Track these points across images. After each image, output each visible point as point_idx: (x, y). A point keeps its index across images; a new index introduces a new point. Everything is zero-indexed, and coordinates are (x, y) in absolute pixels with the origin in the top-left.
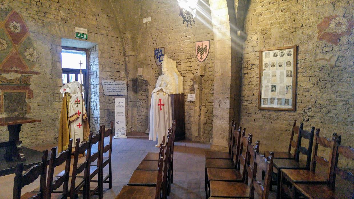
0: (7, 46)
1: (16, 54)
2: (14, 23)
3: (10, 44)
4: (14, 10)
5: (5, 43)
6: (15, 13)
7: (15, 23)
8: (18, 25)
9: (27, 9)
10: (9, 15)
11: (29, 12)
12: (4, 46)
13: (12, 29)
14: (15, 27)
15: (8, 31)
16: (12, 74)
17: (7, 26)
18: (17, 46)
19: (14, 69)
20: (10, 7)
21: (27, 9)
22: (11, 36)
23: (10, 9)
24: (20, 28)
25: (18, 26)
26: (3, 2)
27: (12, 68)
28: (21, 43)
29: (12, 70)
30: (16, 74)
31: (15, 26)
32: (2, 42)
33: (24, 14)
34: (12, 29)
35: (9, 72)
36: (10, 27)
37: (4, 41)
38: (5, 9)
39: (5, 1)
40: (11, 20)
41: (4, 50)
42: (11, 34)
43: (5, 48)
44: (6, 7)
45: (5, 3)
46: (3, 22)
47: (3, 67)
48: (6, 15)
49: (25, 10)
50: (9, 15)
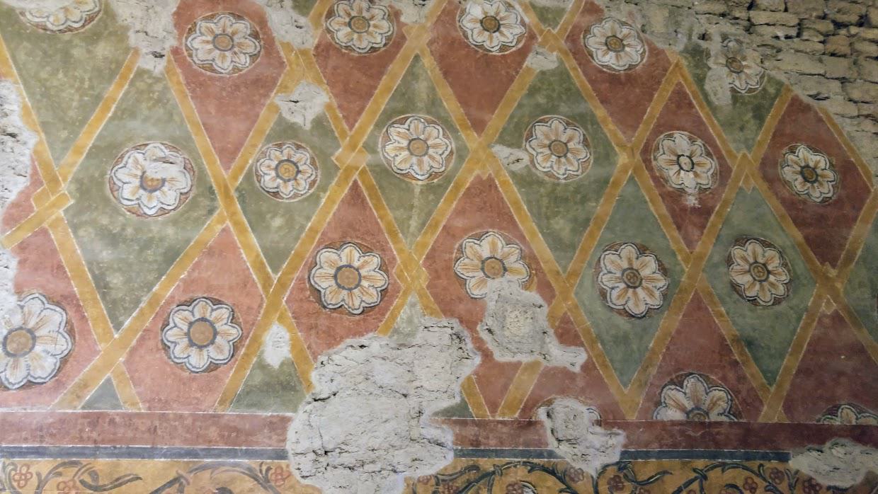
0: (785, 278)
1: (837, 318)
2: (801, 155)
3: (801, 267)
4: (789, 90)
5: (777, 262)
6: (797, 107)
7: (804, 154)
8: (818, 160)
9: (843, 80)
10: (771, 121)
11: (856, 95)
12: (772, 278)
13: (798, 185)
14: (809, 174)
15: (783, 201)
16: (838, 452)
17: (769, 170)
18: (833, 273)
19: (847, 416)
20: (771, 79)
21: (843, 80)
22: (799, 223)
23: (772, 90)
24: (830, 175)
25: (822, 165)
26: (734, 60)
27: (833, 411)
28: (850, 258)
29: (837, 422)
30: (857, 449)
31: (807, 166)
32: (761, 260)
33: (835, 106)
34: (798, 185)
35: (823, 442)
36: (788, 173)
37: (770, 253)
38: (750, 90)
39: (744, 58)
40: (783, 140)
41: (777, 301)
42: (795, 208)
43: (781, 290)
44: (753, 83)
45: (744, 63)
46: (749, 156)
47: (789, 407)
48: (759, 115)
49: (836, 86)
50: (771, 121)
